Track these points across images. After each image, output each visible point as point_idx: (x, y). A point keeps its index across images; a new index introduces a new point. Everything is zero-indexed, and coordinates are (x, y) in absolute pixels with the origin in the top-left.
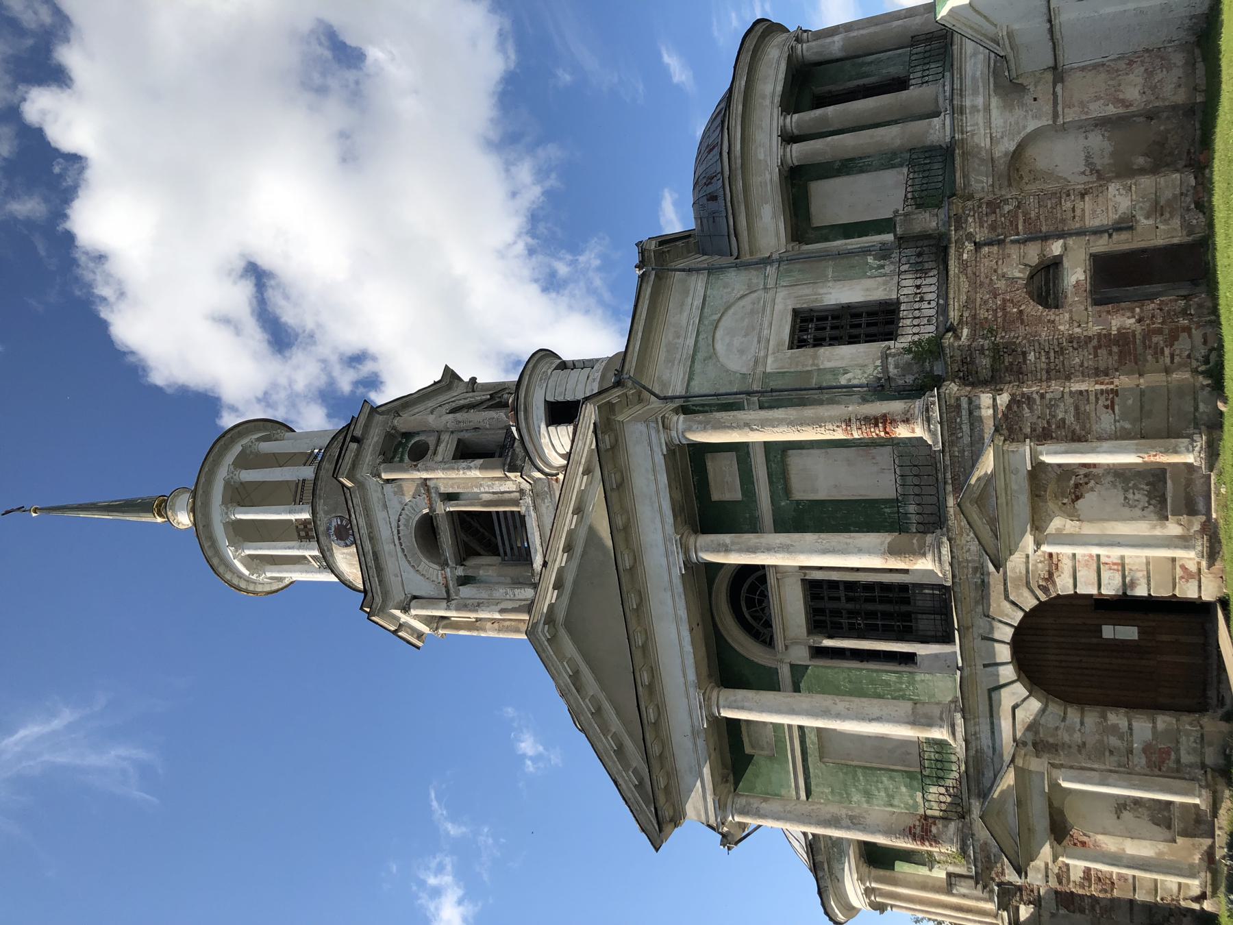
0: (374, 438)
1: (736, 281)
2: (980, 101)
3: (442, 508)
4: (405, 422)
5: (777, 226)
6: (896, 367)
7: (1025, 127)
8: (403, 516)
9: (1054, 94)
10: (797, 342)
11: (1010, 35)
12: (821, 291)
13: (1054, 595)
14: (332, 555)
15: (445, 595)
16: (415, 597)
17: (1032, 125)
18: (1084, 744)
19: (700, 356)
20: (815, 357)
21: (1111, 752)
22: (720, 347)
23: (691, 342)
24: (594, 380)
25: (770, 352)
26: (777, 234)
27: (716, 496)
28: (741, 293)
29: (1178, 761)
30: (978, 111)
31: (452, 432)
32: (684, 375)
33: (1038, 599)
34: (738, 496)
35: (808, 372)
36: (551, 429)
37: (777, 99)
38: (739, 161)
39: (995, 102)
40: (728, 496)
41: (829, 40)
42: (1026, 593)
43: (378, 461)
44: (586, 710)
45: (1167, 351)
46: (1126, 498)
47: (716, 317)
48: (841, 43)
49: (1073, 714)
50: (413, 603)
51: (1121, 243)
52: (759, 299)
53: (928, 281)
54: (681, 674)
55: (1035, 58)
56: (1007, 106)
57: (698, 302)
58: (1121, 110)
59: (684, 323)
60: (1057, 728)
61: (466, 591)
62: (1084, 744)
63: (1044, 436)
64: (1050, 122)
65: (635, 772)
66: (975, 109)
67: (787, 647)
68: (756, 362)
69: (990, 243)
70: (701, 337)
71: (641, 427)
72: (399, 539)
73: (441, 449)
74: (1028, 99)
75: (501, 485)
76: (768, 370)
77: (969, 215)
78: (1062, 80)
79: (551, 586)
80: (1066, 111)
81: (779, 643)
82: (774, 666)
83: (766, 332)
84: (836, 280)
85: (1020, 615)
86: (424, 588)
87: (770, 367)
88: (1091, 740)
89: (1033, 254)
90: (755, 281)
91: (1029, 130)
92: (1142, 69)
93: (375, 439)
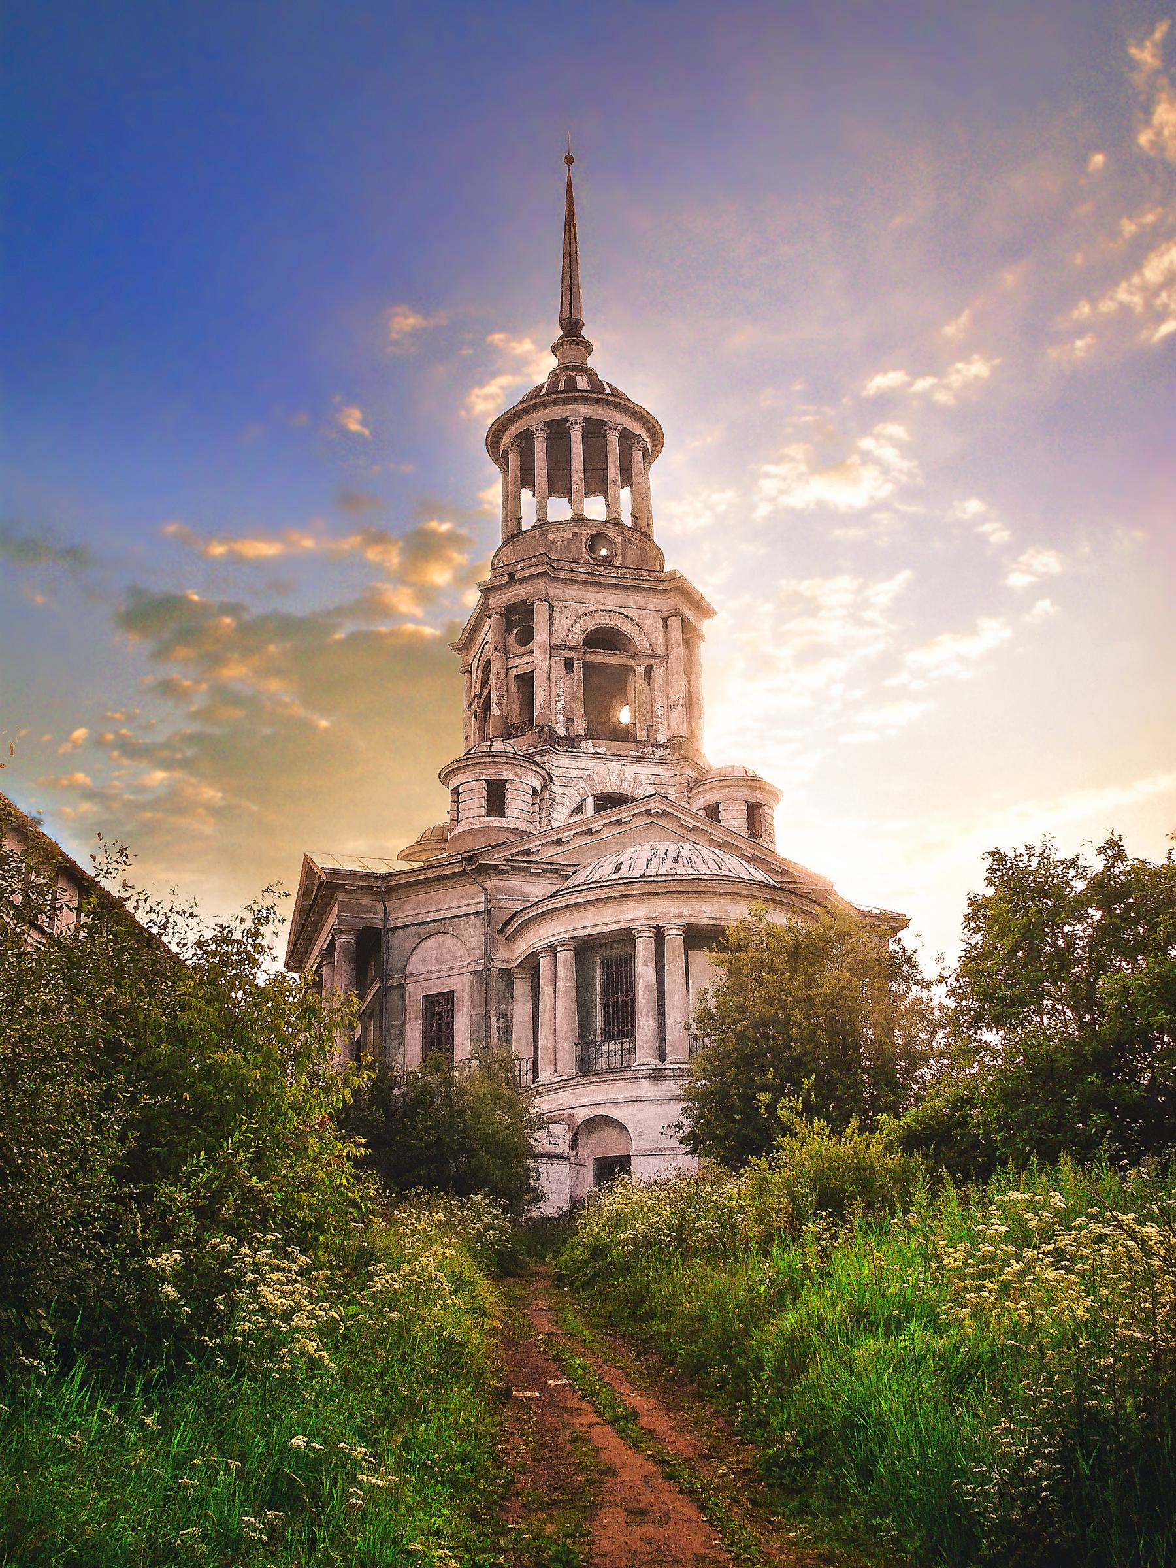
12: (465, 1010)
19: (422, 929)
22: (430, 943)
23: (432, 917)
24: (470, 824)
57: (463, 911)
59: (447, 905)
76: (409, 987)
83: (435, 975)
93: (522, 592)
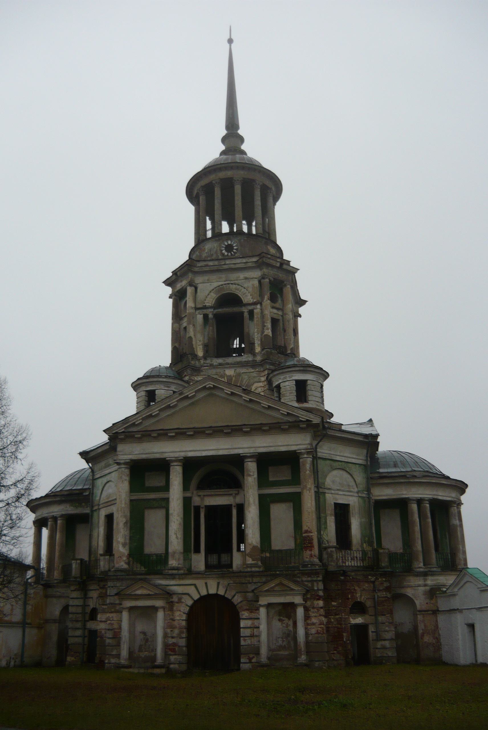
0: (281, 276)
1: (360, 477)
2: (429, 582)
3: (245, 310)
4: (288, 290)
5: (384, 496)
6: (331, 551)
7: (417, 600)
8: (241, 288)
9: (428, 611)
10: (337, 505)
11: (454, 595)
13: (239, 611)
14: (216, 240)
15: (199, 306)
16: (196, 288)
17: (417, 602)
18: (174, 620)
19: (332, 462)
20: (331, 515)
21: (171, 631)
22: (335, 472)
23: (338, 458)
24: (317, 405)
25: (334, 495)
26: (379, 496)
27: (270, 469)
28: (356, 480)
29: (171, 655)
30: (425, 581)
31: (282, 316)
32: (325, 456)
33: (237, 605)
34: (271, 479)
35: (325, 512)
36: (294, 382)
37: (435, 497)
38: (412, 480)
39: (428, 588)
40: (270, 474)
41: (457, 518)
42: (239, 600)
43: (271, 278)
44: (171, 402)
45: (335, 652)
46: (279, 638)
47: (347, 469)
48: (455, 523)
49: (184, 617)
50: (193, 288)
51: (371, 635)
52: (354, 489)
53: (359, 562)
54: (191, 449)
55: (443, 604)
56: (425, 593)
57: (354, 461)
58: (420, 635)
59: (346, 455)
60: (180, 611)
61: (200, 318)
62: (173, 620)
63: (306, 609)
64: (418, 609)
65: (141, 423)
66: (425, 580)
67: (199, 496)
68: (329, 489)
69: (374, 587)
70: (340, 463)
71: (308, 442)
72: (228, 284)
73: (275, 311)
74: (428, 601)
75: (258, 345)
76: (327, 495)
77: (386, 578)
78: (433, 614)
79: (233, 391)
80: (422, 615)
81: (201, 493)
82: (190, 489)
83: (341, 493)
84: (361, 523)
85: (230, 598)
86: (201, 295)
87: (328, 496)
88: (176, 623)
89: (369, 604)
90: (361, 486)
91: (416, 601)
92: (434, 642)
93: (280, 275)
